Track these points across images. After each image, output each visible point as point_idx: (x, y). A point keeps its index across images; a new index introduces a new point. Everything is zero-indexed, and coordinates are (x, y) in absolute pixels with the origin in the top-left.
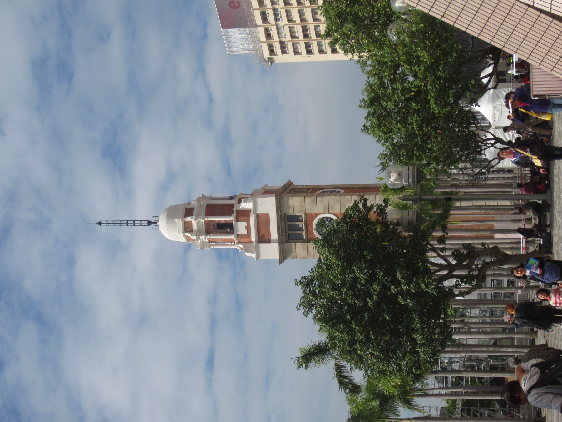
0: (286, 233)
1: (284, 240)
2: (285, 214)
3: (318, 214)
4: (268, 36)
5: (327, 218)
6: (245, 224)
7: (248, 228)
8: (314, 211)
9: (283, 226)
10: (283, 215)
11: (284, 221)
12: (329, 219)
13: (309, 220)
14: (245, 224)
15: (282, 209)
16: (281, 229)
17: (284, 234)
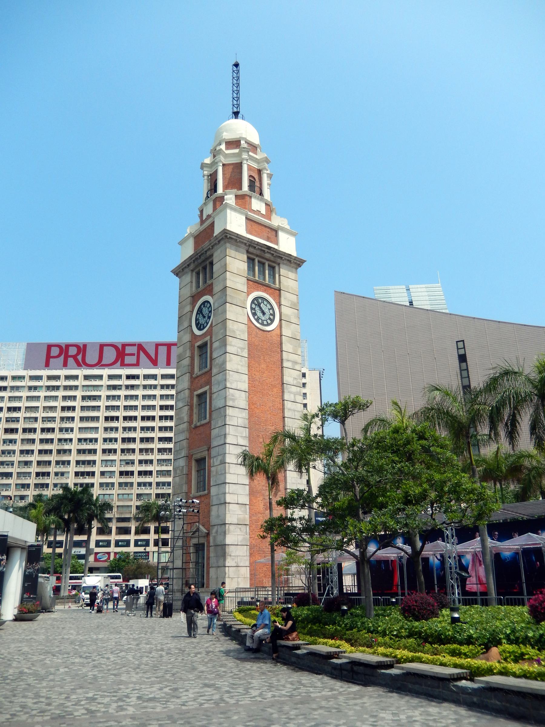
0: (257, 256)
1: (251, 250)
2: (279, 264)
3: (280, 305)
4: (14, 378)
5: (273, 315)
6: (263, 212)
7: (258, 212)
8: (283, 302)
9: (268, 256)
10: (279, 260)
11: (272, 258)
12: (272, 317)
13: (271, 291)
14: (263, 212)
15: (285, 262)
16: (266, 250)
17: (258, 252)
